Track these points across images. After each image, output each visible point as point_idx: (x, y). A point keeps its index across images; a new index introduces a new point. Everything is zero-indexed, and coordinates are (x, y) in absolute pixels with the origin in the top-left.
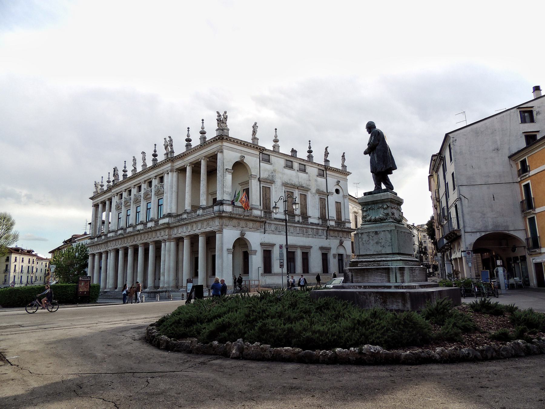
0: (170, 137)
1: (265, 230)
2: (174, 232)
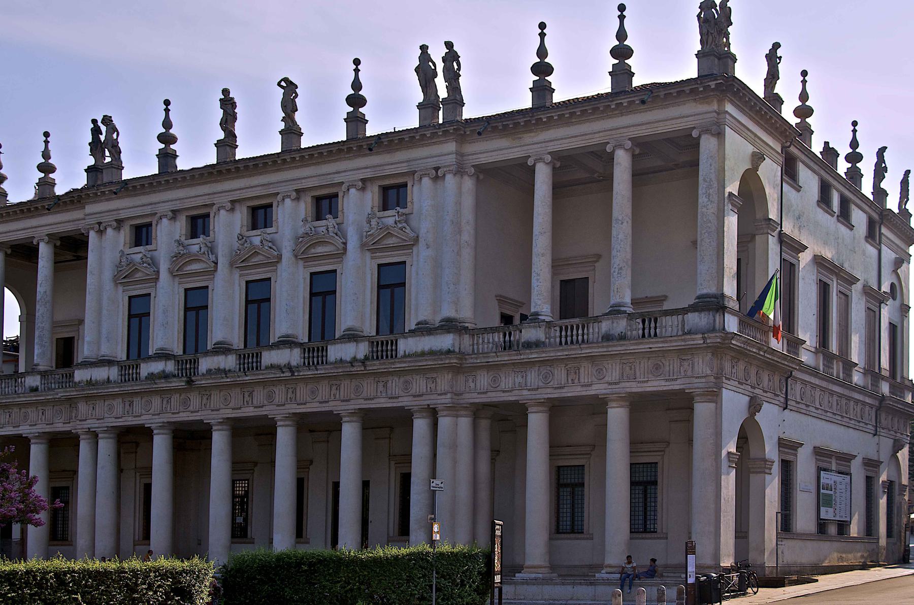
1: (786, 399)
2: (472, 385)
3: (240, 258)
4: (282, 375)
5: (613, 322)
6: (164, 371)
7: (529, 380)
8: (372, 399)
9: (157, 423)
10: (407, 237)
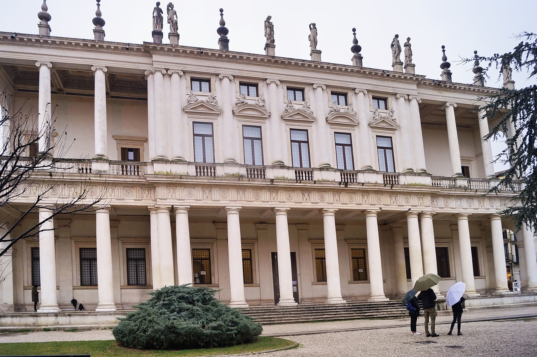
3: (289, 114)
4: (339, 186)
6: (238, 173)
8: (389, 205)
10: (395, 125)
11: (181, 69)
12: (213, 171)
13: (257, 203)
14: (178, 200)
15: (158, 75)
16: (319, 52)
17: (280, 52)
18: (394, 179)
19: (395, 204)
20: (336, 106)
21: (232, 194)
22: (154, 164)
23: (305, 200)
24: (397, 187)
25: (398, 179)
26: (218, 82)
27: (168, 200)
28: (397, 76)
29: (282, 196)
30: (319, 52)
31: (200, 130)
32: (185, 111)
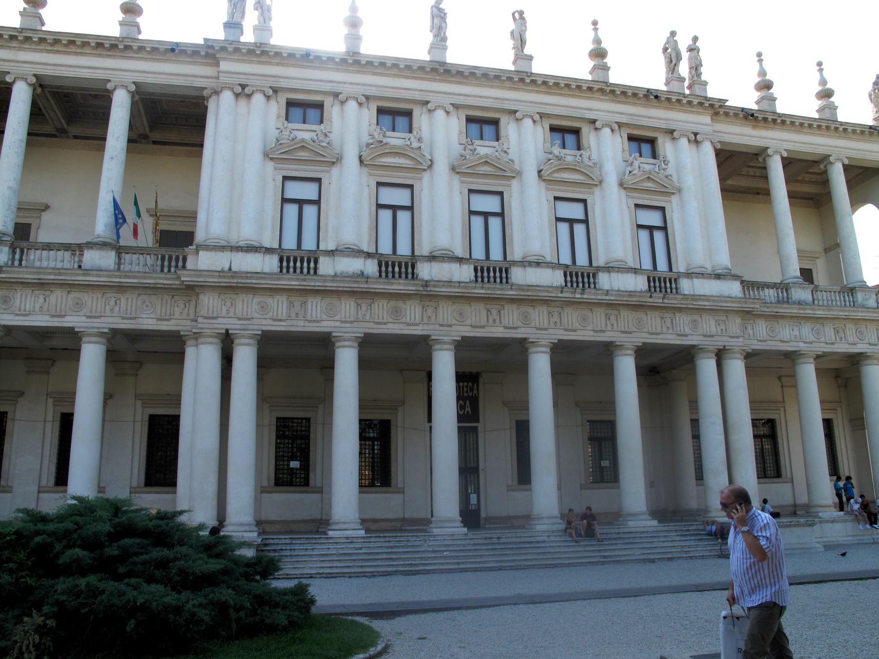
0: (695, 39)
2: (751, 332)
3: (466, 164)
5: (865, 295)
7: (804, 334)
8: (659, 334)
9: (354, 333)
10: (670, 185)
11: (269, 85)
12: (312, 265)
13: (396, 326)
14: (240, 319)
15: (227, 97)
16: (530, 58)
17: (454, 56)
18: (668, 285)
19: (670, 331)
20: (557, 150)
21: (347, 308)
22: (201, 253)
23: (491, 321)
24: (675, 299)
25: (676, 284)
26: (336, 110)
27: (220, 320)
28: (674, 98)
29: (446, 312)
30: (530, 58)
31: (296, 190)
32: (270, 156)
